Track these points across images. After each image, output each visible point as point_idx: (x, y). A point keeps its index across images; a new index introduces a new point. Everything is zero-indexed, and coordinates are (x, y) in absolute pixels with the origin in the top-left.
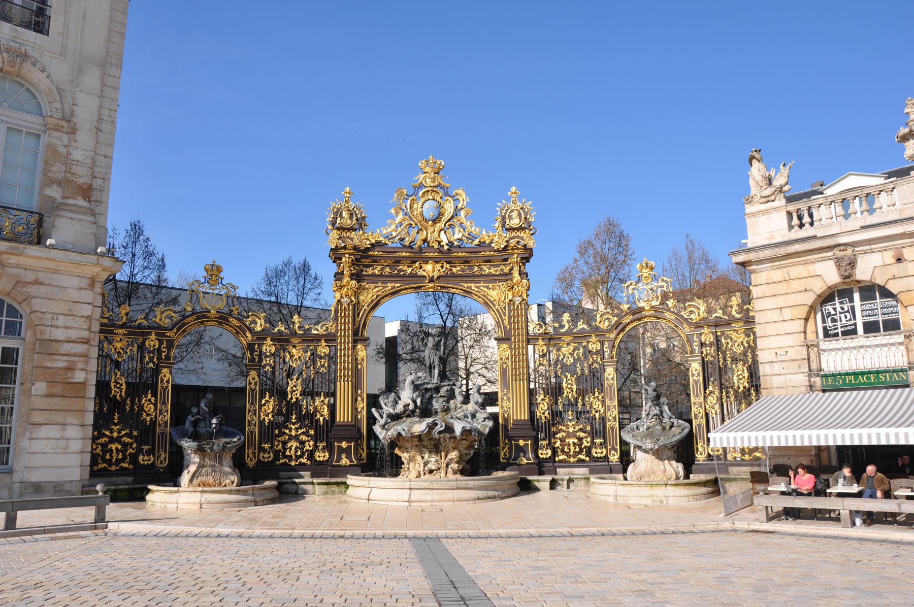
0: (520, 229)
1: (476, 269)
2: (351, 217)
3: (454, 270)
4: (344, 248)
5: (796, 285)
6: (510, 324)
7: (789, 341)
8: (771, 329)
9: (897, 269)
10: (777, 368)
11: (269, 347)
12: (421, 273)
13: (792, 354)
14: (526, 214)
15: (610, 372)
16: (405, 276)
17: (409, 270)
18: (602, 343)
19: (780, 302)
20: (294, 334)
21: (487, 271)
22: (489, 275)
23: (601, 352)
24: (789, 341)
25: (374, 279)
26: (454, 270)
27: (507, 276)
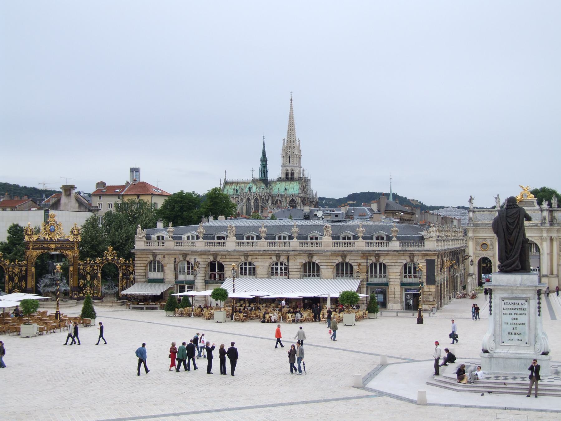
0: (77, 235)
1: (64, 246)
2: (31, 232)
3: (59, 246)
4: (30, 241)
5: (144, 259)
6: (73, 261)
7: (142, 271)
8: (138, 268)
9: (163, 259)
10: (139, 277)
11: (11, 269)
12: (49, 247)
13: (142, 274)
14: (79, 231)
15: (99, 274)
16: (45, 248)
17: (46, 246)
18: (98, 267)
19: (141, 262)
20: (16, 265)
21: (67, 246)
22: (68, 248)
23: (97, 269)
24: (142, 271)
25: (36, 249)
26: (59, 246)
27: (73, 249)
